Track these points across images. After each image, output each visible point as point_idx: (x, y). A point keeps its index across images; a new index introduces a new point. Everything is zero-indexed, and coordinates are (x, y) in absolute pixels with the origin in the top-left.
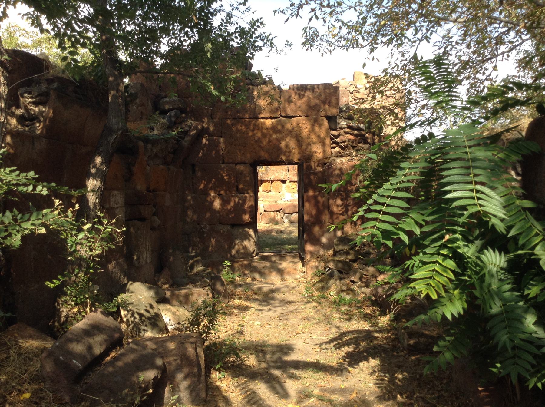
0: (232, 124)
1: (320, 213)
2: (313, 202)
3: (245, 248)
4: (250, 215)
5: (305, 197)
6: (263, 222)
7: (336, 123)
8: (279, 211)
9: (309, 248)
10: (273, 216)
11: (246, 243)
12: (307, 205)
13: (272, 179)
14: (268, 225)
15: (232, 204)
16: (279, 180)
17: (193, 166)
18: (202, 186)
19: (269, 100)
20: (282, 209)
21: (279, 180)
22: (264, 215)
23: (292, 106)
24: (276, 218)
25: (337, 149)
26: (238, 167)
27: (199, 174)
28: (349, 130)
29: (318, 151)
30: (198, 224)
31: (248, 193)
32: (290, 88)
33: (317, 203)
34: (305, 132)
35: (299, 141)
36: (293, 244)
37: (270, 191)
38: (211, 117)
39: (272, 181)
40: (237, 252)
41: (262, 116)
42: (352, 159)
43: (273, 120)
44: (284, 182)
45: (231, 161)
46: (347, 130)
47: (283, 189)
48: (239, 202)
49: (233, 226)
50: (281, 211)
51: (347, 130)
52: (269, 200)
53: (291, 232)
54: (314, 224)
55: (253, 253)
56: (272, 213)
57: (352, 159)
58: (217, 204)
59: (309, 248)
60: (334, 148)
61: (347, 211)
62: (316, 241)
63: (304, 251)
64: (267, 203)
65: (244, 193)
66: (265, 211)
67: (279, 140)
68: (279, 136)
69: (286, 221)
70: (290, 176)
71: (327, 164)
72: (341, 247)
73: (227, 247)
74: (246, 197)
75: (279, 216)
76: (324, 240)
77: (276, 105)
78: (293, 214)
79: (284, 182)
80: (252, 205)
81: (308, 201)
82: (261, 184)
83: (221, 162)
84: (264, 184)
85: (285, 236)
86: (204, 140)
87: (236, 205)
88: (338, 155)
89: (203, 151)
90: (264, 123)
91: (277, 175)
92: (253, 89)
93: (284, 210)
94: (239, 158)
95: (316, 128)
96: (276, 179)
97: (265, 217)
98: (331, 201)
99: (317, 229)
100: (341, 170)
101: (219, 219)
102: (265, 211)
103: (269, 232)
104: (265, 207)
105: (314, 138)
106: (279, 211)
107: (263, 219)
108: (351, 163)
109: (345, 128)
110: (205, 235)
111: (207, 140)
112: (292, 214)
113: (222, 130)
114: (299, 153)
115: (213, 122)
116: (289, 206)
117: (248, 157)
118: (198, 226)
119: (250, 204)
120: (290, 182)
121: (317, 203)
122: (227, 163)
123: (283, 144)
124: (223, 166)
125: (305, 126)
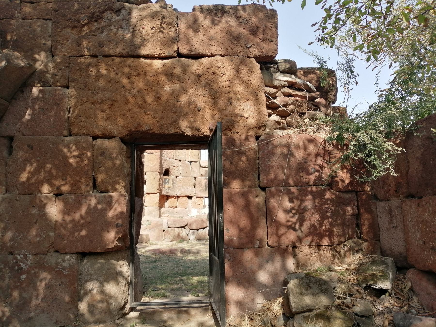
0: (89, 65)
1: (254, 224)
2: (241, 202)
3: (107, 297)
4: (117, 233)
5: (225, 196)
6: (166, 240)
7: (272, 79)
8: (183, 227)
9: (234, 293)
10: (177, 233)
11: (111, 288)
12: (229, 208)
13: (178, 195)
14: (171, 243)
15: (83, 210)
16: (186, 196)
17: (11, 139)
18: (24, 177)
19: (157, 23)
20: (187, 225)
21: (186, 196)
22: (167, 231)
23: (201, 36)
24: (181, 235)
25: (275, 118)
26: (99, 141)
27: (20, 154)
28: (291, 91)
29: (248, 111)
30: (11, 253)
31: (115, 190)
32: (194, 9)
33: (247, 206)
34: (224, 81)
35: (215, 97)
36: (199, 275)
37: (176, 207)
38: (52, 53)
39: (178, 197)
40: (91, 307)
41: (144, 51)
42: (303, 131)
43: (165, 61)
44: (190, 198)
45: (84, 131)
46: (287, 90)
47: (190, 205)
48: (95, 207)
49: (83, 255)
50: (186, 227)
51: (287, 90)
52: (175, 216)
53: (198, 252)
54: (241, 247)
55: (124, 307)
56: (176, 229)
57: (303, 131)
58: (54, 210)
59: (234, 293)
60: (269, 115)
61: (302, 221)
62: (247, 280)
63: (223, 302)
64: (172, 218)
65: (107, 191)
66: (168, 227)
67: (176, 95)
68: (177, 87)
69: (192, 237)
70: (197, 192)
71: (262, 138)
72: (308, 300)
73: (67, 299)
74: (111, 197)
75: (184, 232)
76: (263, 277)
77: (171, 32)
78: (200, 230)
79: (190, 198)
80: (122, 213)
81: (230, 200)
82: (167, 199)
83: (65, 132)
84: (170, 200)
85: (191, 257)
86: (35, 91)
87: (91, 211)
88: (278, 126)
89: (33, 109)
90: (150, 65)
91: (183, 191)
92: (130, 9)
93: (190, 225)
94: (102, 124)
95: (244, 71)
96: (183, 195)
97: (169, 234)
98: (273, 202)
99: (248, 256)
100: (288, 146)
101: (56, 242)
102: (168, 227)
103: (172, 252)
104: (169, 223)
105: (239, 88)
106: (183, 227)
107: (166, 236)
108: (304, 136)
109: (284, 86)
110: (24, 277)
111: (40, 91)
112: (198, 230)
113: (71, 73)
114: (213, 116)
115: (55, 61)
116: (196, 221)
117: (120, 125)
118: (10, 257)
119: (119, 210)
120: (197, 198)
121: (247, 207)
122: (76, 135)
123: (183, 99)
124: (68, 138)
125: (225, 68)
